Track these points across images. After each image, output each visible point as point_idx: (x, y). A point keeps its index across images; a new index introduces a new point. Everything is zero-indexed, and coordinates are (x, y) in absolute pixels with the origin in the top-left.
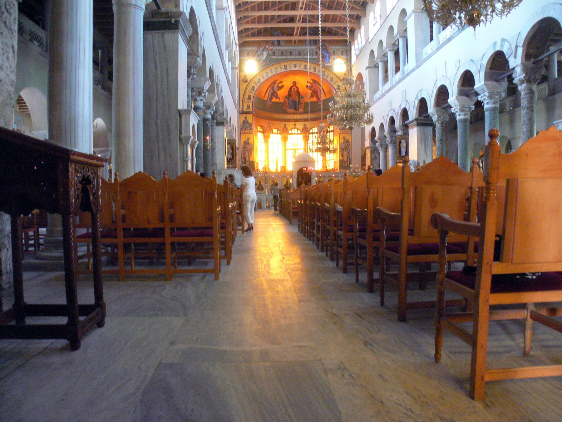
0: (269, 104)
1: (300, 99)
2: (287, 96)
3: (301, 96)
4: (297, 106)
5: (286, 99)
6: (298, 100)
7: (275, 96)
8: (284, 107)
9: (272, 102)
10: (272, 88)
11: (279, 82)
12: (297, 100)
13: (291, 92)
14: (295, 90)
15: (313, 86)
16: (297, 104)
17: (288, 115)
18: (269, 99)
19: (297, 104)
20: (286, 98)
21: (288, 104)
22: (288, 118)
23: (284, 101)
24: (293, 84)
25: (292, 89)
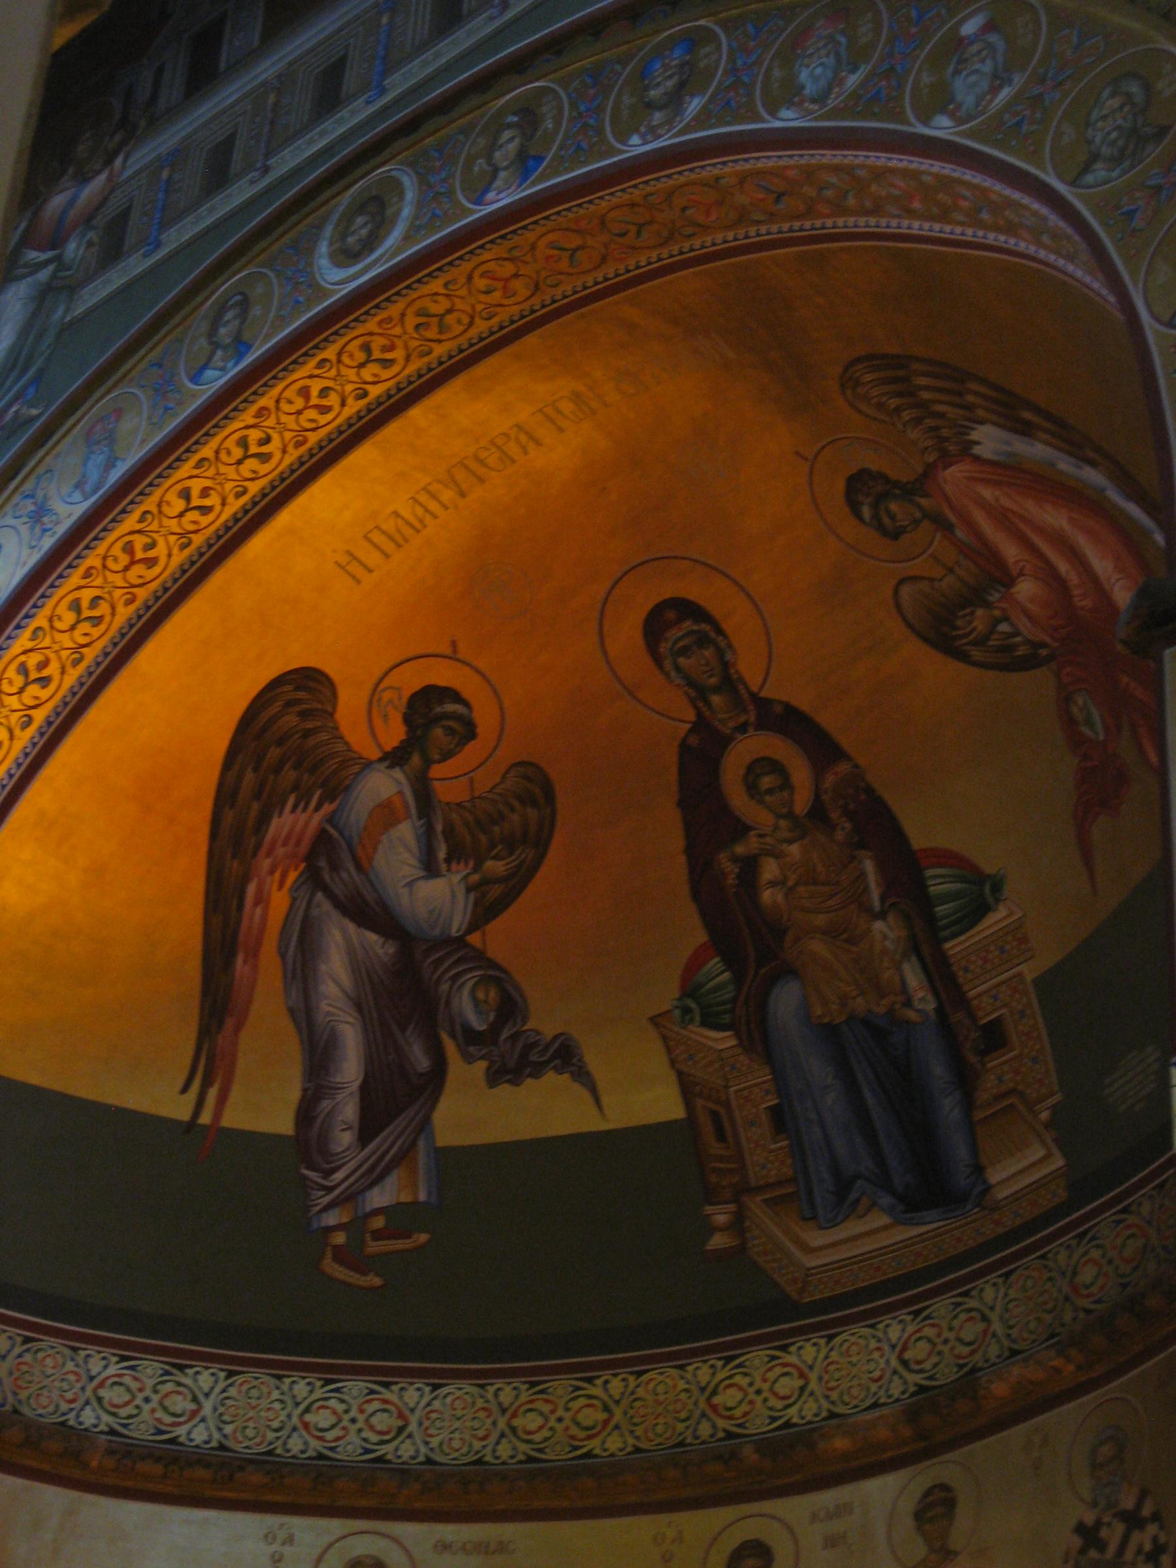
0: (379, 1197)
1: (954, 947)
2: (716, 971)
3: (939, 882)
4: (949, 1107)
5: (723, 1040)
6: (913, 976)
7: (470, 1039)
8: (721, 1216)
9: (443, 1155)
10: (313, 879)
11: (394, 733)
12: (924, 1001)
13: (750, 866)
14: (802, 801)
15: (1011, 552)
16: (938, 1071)
17: (808, 1351)
18: (350, 1111)
19: (938, 1071)
20: (710, 1021)
21: (780, 1119)
22: (807, 1410)
23: (688, 1089)
24: (698, 692)
25: (738, 799)
